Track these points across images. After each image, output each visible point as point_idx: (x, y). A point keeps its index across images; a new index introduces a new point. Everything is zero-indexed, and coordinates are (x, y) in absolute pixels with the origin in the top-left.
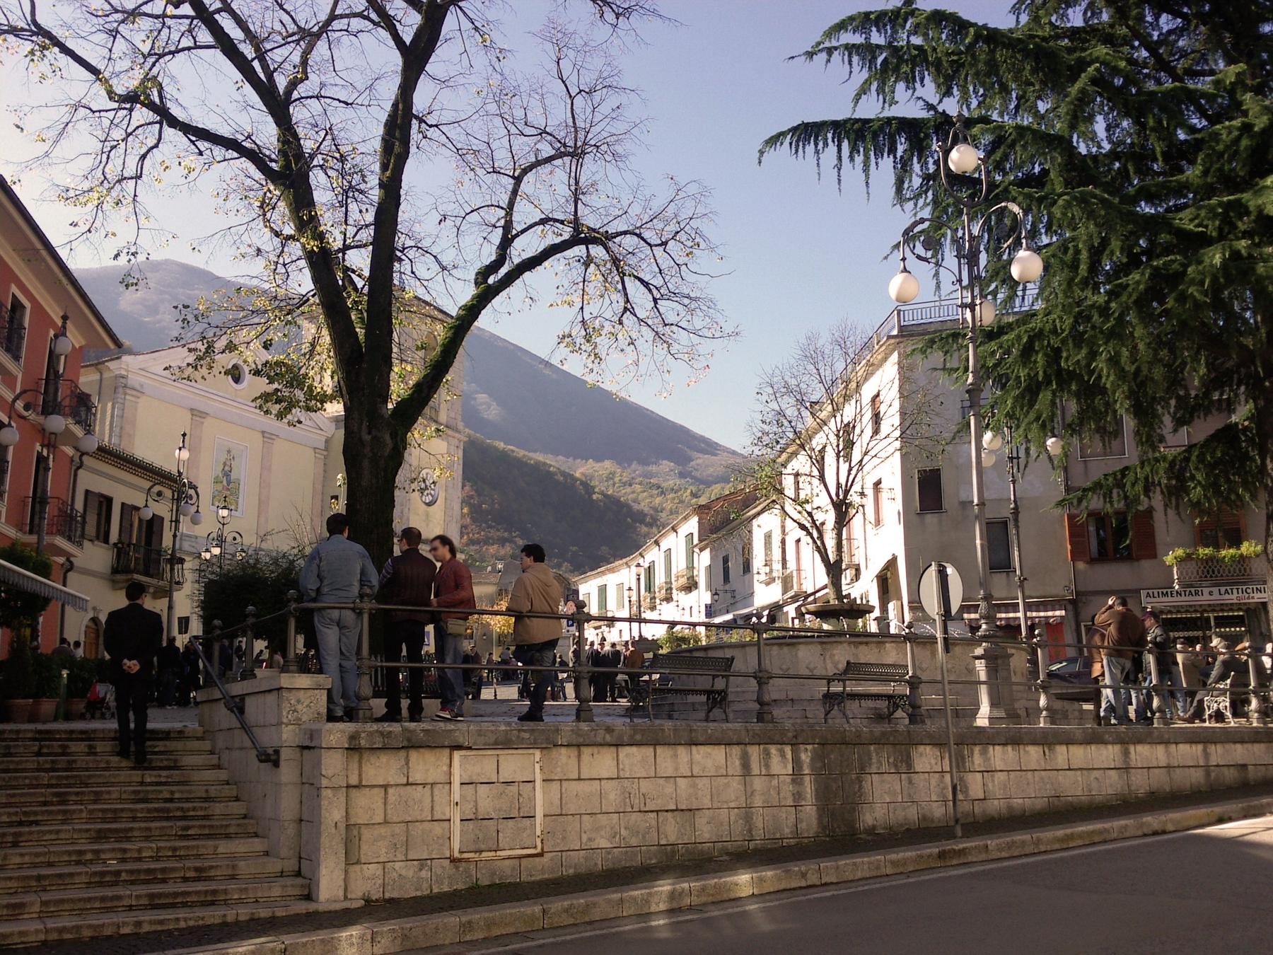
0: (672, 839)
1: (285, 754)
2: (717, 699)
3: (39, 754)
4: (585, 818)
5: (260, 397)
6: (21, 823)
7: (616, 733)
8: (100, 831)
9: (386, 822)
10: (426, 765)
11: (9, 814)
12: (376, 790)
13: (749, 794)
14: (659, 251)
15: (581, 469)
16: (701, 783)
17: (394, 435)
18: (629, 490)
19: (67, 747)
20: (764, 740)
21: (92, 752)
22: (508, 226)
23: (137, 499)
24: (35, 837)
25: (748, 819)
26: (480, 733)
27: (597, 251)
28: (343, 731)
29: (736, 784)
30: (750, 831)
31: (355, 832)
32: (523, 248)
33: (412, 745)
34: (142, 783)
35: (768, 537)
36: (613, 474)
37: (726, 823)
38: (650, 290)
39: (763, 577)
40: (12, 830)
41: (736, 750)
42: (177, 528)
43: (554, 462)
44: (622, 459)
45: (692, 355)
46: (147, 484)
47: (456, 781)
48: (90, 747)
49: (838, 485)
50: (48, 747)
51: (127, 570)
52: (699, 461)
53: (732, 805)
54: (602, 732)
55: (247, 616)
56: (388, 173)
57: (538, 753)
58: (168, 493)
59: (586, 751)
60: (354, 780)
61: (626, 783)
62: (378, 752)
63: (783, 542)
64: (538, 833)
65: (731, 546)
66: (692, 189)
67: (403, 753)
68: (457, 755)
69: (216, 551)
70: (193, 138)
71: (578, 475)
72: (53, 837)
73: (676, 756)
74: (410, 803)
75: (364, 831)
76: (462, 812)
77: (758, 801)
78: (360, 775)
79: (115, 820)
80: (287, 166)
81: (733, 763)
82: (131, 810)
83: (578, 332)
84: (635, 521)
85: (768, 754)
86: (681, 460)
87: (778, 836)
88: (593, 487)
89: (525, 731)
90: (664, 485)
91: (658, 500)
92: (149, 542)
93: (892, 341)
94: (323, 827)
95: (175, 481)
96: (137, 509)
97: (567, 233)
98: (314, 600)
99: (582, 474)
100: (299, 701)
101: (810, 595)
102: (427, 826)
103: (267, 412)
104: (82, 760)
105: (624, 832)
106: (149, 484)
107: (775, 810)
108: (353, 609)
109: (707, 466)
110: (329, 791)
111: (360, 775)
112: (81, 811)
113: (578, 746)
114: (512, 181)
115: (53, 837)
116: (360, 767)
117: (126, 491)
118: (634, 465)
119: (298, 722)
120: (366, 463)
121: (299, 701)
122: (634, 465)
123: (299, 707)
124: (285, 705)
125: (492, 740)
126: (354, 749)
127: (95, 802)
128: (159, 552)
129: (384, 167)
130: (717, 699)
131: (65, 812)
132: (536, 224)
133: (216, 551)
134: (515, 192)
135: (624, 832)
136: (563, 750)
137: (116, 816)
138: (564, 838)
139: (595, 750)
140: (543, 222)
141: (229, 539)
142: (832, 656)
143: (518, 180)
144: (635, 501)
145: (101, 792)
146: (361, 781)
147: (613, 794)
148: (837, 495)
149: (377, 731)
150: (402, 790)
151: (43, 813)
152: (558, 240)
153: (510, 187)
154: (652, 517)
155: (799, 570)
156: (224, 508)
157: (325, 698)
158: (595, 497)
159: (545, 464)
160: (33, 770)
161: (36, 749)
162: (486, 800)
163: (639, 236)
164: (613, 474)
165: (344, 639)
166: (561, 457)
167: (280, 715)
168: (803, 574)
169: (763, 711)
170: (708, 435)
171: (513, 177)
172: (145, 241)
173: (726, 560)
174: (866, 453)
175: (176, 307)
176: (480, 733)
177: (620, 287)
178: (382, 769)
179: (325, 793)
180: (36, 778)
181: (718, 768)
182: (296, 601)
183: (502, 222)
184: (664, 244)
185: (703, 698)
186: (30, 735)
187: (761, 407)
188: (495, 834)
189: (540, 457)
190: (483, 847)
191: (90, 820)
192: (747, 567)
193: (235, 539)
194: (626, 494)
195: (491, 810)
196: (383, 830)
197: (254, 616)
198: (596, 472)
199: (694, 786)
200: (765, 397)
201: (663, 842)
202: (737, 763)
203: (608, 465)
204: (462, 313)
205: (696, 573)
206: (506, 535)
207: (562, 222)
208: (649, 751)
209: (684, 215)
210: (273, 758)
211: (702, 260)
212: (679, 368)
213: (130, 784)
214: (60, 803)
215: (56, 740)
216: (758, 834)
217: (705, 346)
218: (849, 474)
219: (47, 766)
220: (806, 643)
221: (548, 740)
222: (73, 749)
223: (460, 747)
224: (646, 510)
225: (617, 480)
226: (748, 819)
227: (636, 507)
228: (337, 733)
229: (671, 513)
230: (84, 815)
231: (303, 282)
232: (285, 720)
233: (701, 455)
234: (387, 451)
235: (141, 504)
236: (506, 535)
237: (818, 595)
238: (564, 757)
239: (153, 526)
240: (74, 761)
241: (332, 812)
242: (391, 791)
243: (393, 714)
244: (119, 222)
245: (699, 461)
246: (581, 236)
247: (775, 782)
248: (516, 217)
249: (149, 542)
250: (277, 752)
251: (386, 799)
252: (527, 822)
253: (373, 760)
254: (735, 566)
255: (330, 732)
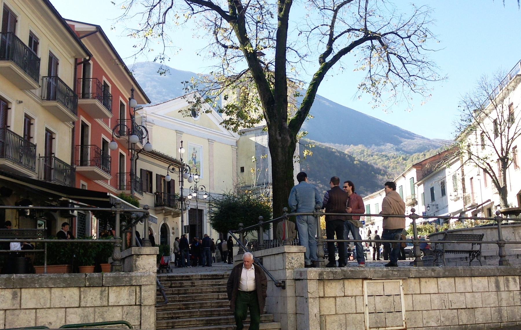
0: (465, 322)
1: (288, 283)
2: (474, 255)
3: (171, 287)
4: (424, 312)
5: (223, 122)
6: (172, 318)
7: (436, 272)
8: (207, 320)
9: (336, 314)
10: (352, 287)
11: (168, 314)
12: (331, 299)
13: (500, 300)
14: (406, 41)
15: (348, 150)
16: (477, 295)
17: (291, 136)
18: (371, 158)
19: (183, 283)
20: (506, 274)
21: (193, 285)
22: (331, 35)
23: (164, 172)
24: (180, 324)
25: (500, 312)
26: (375, 272)
27: (376, 43)
28: (316, 272)
29: (493, 296)
30: (501, 318)
31: (323, 319)
32: (339, 46)
33: (346, 278)
34: (218, 299)
35: (454, 177)
36: (363, 151)
37: (489, 314)
38: (401, 60)
39: (453, 197)
40: (172, 321)
41: (493, 279)
42: (182, 185)
43: (335, 147)
44: (367, 144)
45: (423, 90)
46: (167, 166)
47: (366, 295)
48: (192, 283)
49: (502, 149)
50: (174, 283)
51: (161, 205)
52: (405, 143)
53: (492, 306)
54: (430, 271)
55: (259, 220)
56: (282, 13)
57: (401, 281)
58: (177, 169)
59: (423, 280)
60: (322, 295)
61: (442, 296)
62: (331, 281)
63: (463, 180)
64: (404, 319)
65: (435, 183)
66: (424, 9)
67: (341, 282)
68: (365, 282)
69: (195, 195)
70: (189, 3)
71: (346, 152)
72: (188, 323)
73: (464, 282)
74: (346, 305)
75: (327, 318)
76: (369, 309)
77: (504, 304)
78: (324, 292)
79: (211, 315)
80: (234, 13)
81: (491, 285)
82: (218, 311)
83: (369, 83)
84: (376, 173)
85: (508, 281)
86: (396, 142)
87: (514, 320)
88: (354, 158)
89: (395, 271)
90: (389, 155)
91: (386, 163)
92: (169, 191)
93: (518, 77)
94: (310, 317)
95: (179, 163)
96: (164, 177)
97: (362, 35)
98: (296, 211)
99: (348, 152)
100: (292, 258)
101: (480, 206)
102: (354, 315)
103: (228, 129)
104: (191, 289)
105: (442, 319)
106: (167, 166)
107: (512, 308)
108: (313, 215)
109: (410, 145)
110: (311, 299)
111: (324, 292)
112: (197, 311)
113: (419, 278)
114: (333, 12)
115: (188, 323)
116: (324, 289)
117: (158, 169)
118: (373, 146)
119: (292, 268)
120: (280, 150)
121: (292, 258)
122: (373, 146)
123: (293, 261)
124: (287, 260)
125: (381, 275)
126: (321, 280)
127: (201, 307)
128: (174, 196)
129: (280, 10)
130: (474, 255)
131: (190, 312)
132: (345, 32)
133: (195, 195)
134: (335, 17)
135: (442, 319)
136: (412, 280)
137: (212, 313)
138: (415, 322)
139: (427, 280)
140: (349, 30)
141: (200, 189)
142: (519, 233)
143: (336, 11)
144: (375, 163)
145: (203, 303)
146: (324, 295)
147: (436, 302)
148: (502, 154)
149: (331, 271)
150: (342, 298)
151: (181, 313)
152: (357, 39)
153: (333, 15)
154: (384, 171)
155: (472, 193)
156: (196, 175)
157: (303, 257)
158: (355, 162)
159: (330, 148)
160: (171, 294)
161: (169, 285)
162: (380, 304)
163: (396, 34)
164: (363, 151)
165: (310, 229)
166: (337, 144)
167: (284, 265)
168: (475, 195)
169: (502, 259)
170: (409, 130)
171: (334, 10)
172: (168, 53)
173: (432, 190)
174: (515, 134)
175: (182, 83)
176: (375, 272)
177: (386, 59)
178: (333, 289)
179: (311, 300)
180: (174, 298)
181: (485, 288)
182: (287, 212)
183: (329, 33)
184: (409, 37)
185: (468, 255)
186: (165, 279)
187: (460, 113)
188: (384, 320)
189: (327, 145)
190: (379, 325)
191: (201, 316)
192: (444, 193)
193: (202, 189)
194: (370, 160)
195: (382, 308)
196: (335, 318)
197: (262, 220)
198: (356, 151)
199: (474, 297)
200: (462, 108)
201: (461, 323)
202: (494, 285)
203: (360, 146)
204: (315, 77)
205: (416, 197)
206: (314, 183)
207: (359, 30)
208: (452, 280)
209: (419, 22)
210: (283, 285)
211: (430, 43)
212: (417, 96)
213: (213, 299)
214: (186, 309)
215: (178, 280)
216: (505, 319)
217: (430, 85)
218: (508, 143)
219: (177, 292)
220: (505, 227)
221: (406, 275)
222: (185, 284)
223: (366, 279)
224: (381, 168)
225: (365, 154)
226: (500, 312)
227: (375, 166)
228: (313, 273)
229: (393, 169)
230: (198, 314)
231: (243, 65)
232: (287, 267)
233: (406, 140)
234: (289, 144)
235: (165, 175)
236: (314, 183)
237: (484, 205)
238: (413, 283)
239: (170, 185)
240: (188, 289)
241: (314, 309)
242: (338, 299)
243: (332, 264)
244: (156, 45)
245: (405, 143)
246: (369, 36)
247: (512, 294)
248: (335, 30)
249: (169, 191)
250: (284, 282)
251: (336, 303)
252: (398, 314)
253: (329, 284)
254: (437, 192)
255: (311, 272)
